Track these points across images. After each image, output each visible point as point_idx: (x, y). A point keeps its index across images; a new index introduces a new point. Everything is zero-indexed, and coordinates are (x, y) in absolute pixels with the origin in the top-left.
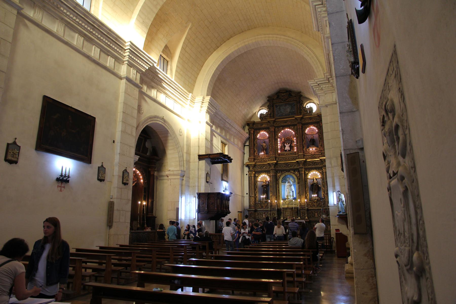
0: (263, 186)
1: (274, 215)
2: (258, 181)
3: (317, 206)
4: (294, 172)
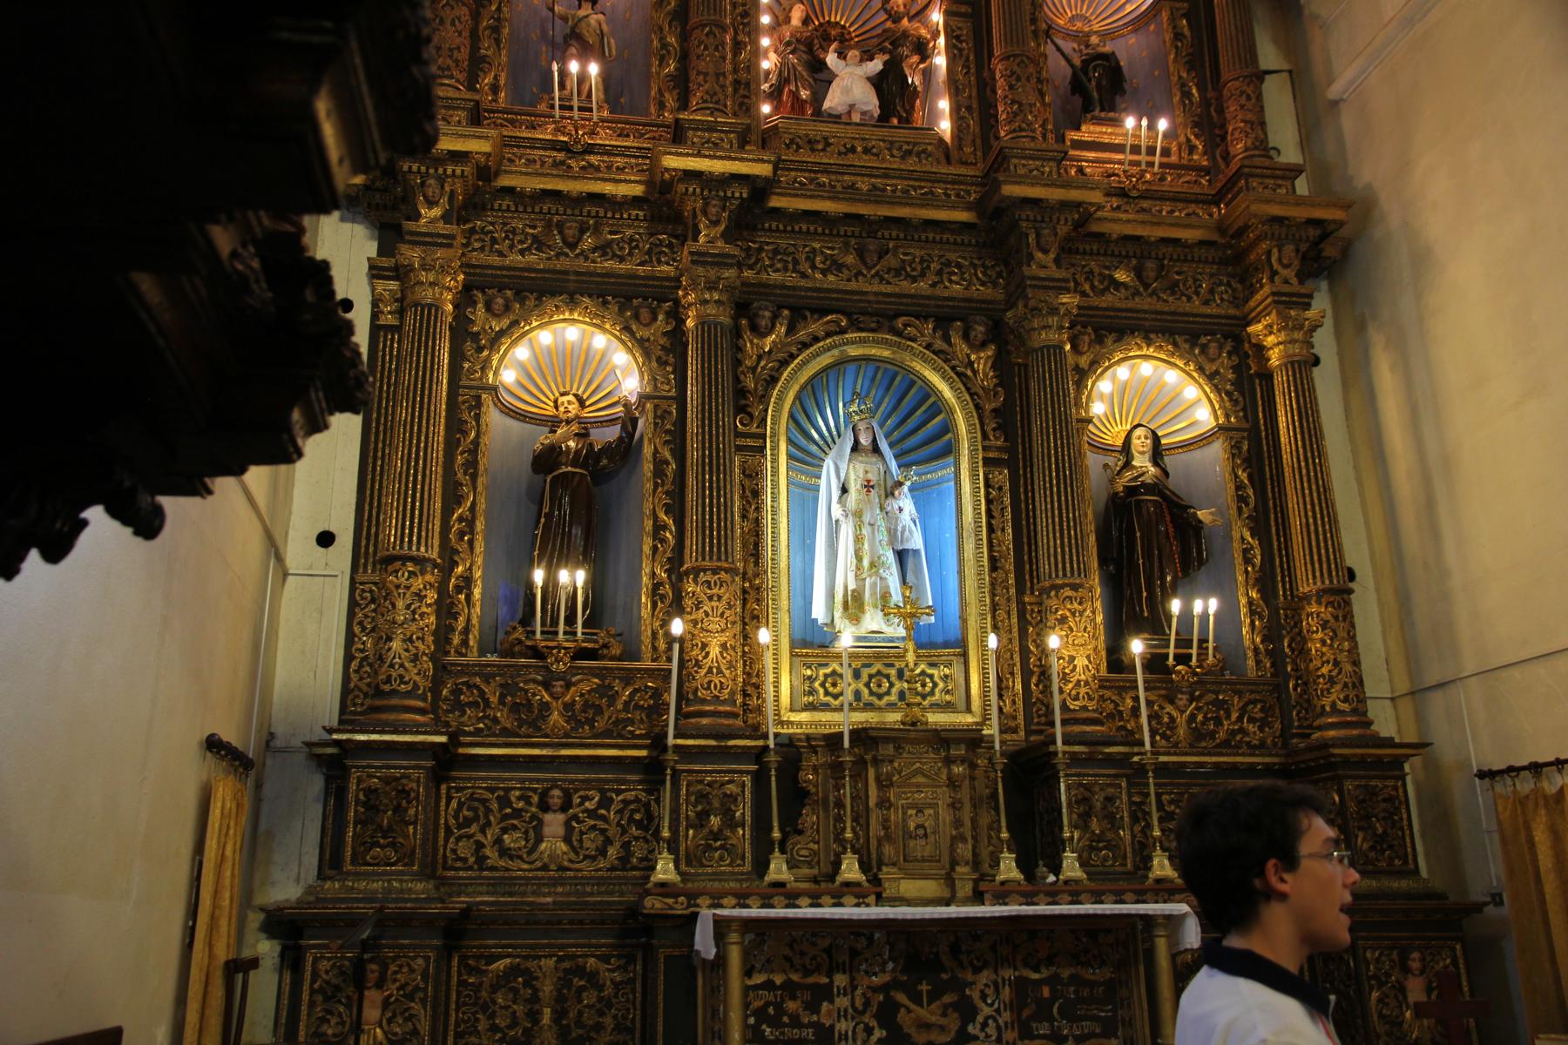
0: (546, 460)
1: (715, 821)
2: (494, 389)
3: (1198, 735)
4: (939, 344)
